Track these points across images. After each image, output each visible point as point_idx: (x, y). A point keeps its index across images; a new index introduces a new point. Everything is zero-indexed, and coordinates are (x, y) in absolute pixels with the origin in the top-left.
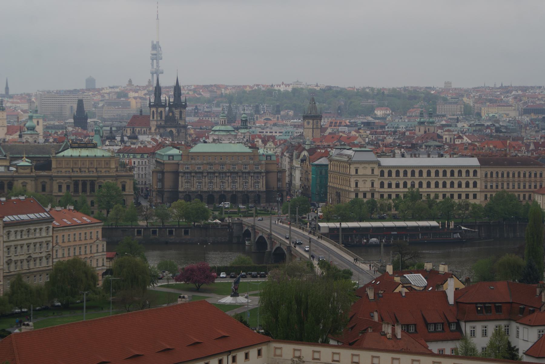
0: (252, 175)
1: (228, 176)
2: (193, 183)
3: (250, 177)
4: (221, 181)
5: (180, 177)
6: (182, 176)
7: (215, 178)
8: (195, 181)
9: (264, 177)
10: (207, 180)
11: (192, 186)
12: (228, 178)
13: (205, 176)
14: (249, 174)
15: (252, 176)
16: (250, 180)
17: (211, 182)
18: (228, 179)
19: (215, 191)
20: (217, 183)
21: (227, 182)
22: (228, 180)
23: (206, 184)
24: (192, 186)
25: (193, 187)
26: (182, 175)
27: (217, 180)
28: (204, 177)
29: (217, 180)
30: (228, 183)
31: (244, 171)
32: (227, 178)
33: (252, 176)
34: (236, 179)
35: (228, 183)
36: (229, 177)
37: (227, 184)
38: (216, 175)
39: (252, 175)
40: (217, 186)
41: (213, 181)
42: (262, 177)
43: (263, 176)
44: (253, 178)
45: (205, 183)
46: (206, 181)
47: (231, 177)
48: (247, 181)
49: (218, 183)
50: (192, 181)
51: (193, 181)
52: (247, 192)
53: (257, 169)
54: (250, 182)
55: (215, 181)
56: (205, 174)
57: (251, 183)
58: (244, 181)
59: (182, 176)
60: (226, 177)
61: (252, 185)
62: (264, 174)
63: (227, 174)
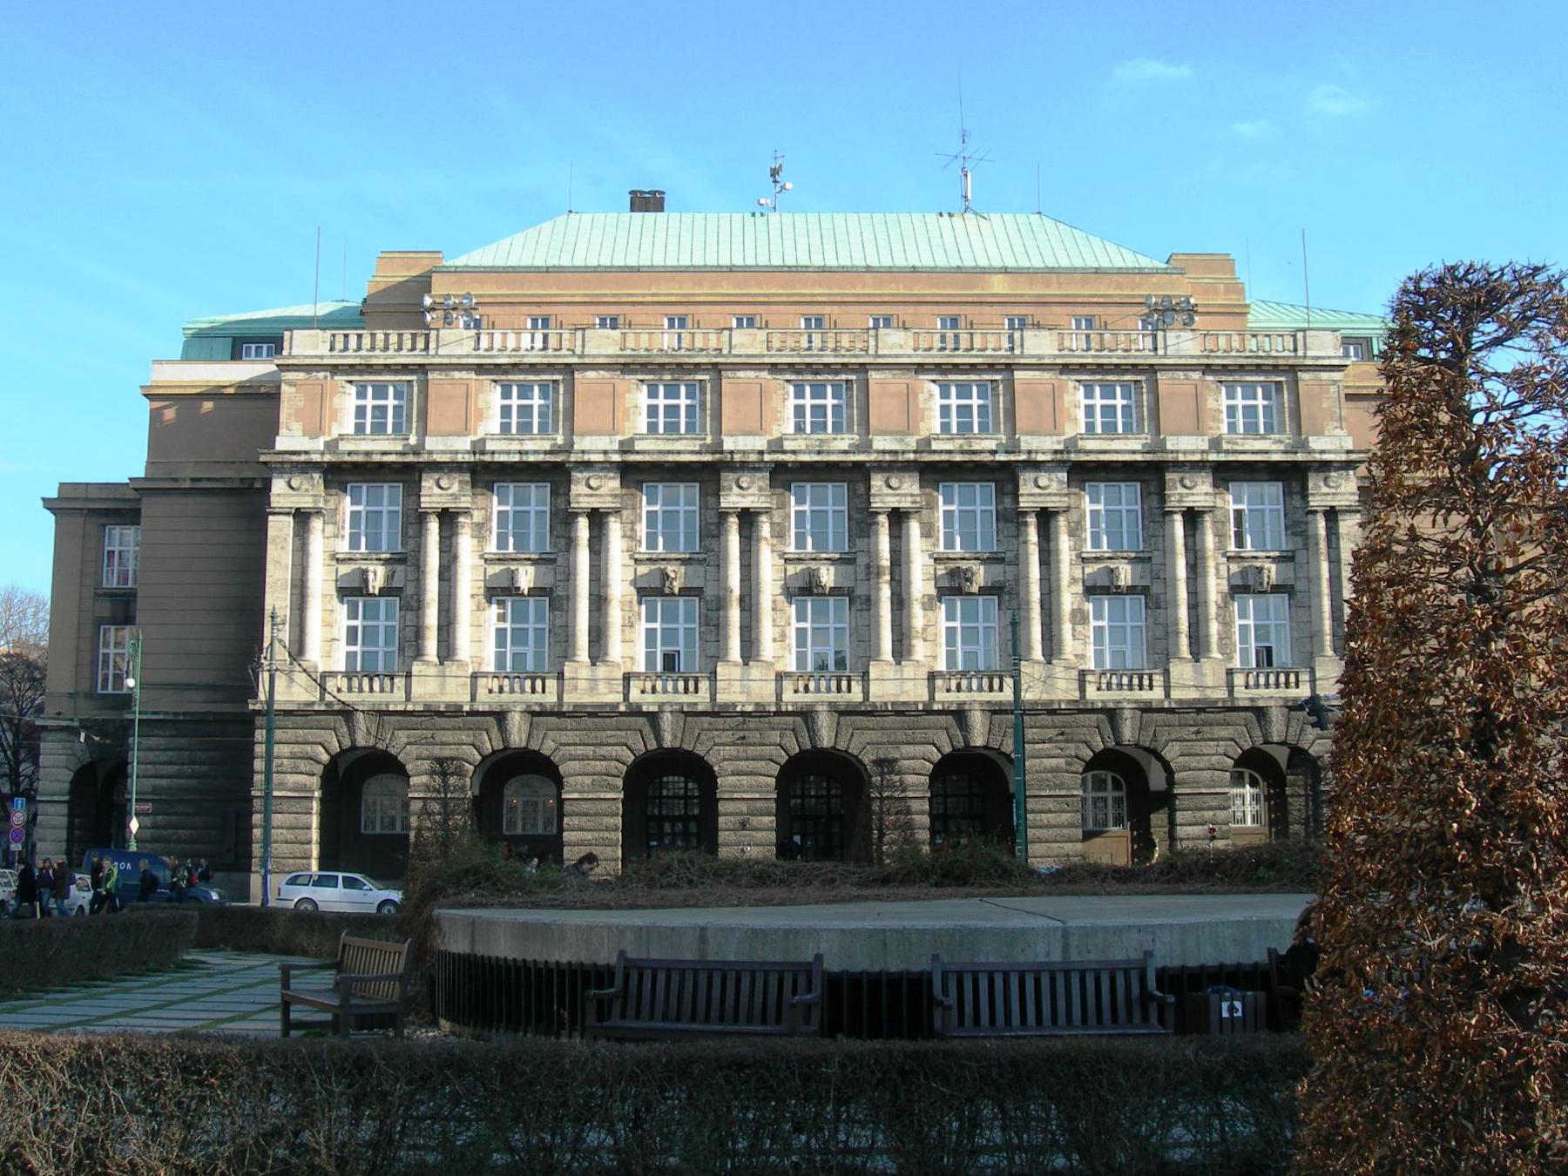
0: (1199, 492)
1: (898, 518)
5: (280, 529)
6: (302, 518)
11: (431, 645)
14: (1162, 486)
19: (719, 712)
24: (431, 645)
25: (447, 651)
26: (306, 502)
28: (583, 528)
35: (900, 602)
36: (914, 527)
38: (733, 499)
39: (1199, 492)
43: (1332, 514)
52: (1146, 708)
63: (877, 482)
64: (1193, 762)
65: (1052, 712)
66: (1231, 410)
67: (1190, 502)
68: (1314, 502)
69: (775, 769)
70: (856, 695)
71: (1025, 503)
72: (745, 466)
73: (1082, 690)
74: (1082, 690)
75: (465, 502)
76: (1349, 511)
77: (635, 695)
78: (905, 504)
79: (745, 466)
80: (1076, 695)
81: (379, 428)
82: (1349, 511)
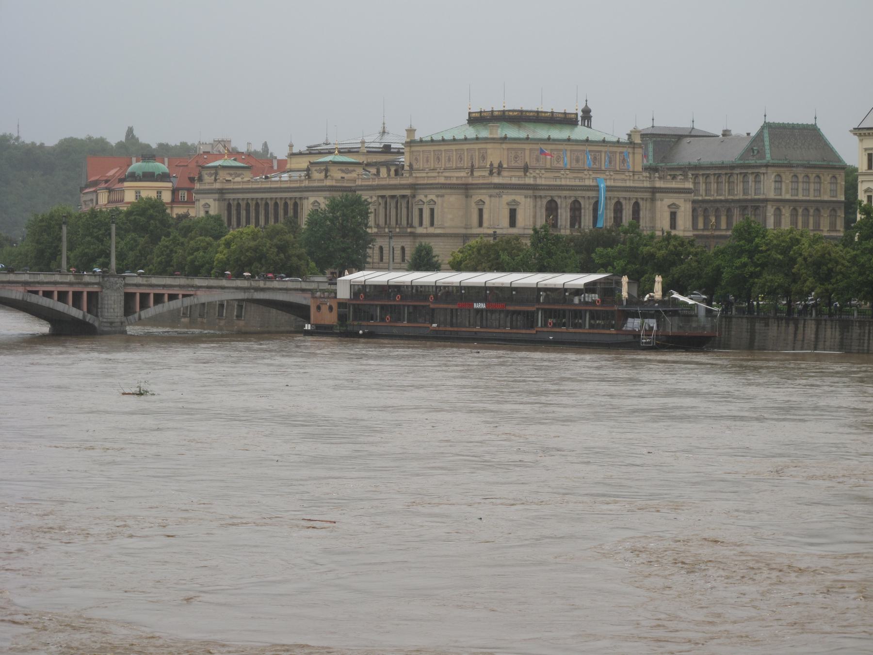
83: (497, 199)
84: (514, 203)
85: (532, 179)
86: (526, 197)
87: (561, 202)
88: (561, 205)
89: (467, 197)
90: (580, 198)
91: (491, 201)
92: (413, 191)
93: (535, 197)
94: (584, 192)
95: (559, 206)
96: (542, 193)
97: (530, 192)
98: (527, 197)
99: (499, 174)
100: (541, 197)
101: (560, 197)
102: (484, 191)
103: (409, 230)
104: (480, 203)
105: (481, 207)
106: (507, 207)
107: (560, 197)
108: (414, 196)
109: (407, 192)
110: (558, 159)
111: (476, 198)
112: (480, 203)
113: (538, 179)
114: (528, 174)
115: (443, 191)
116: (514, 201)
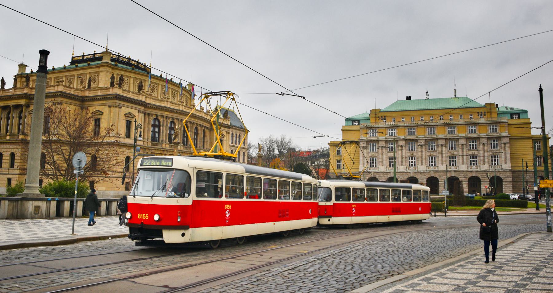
1: (442, 145)
2: (382, 158)
3: (481, 146)
4: (429, 154)
7: (419, 149)
8: (384, 154)
9: (508, 145)
10: (406, 153)
12: (442, 148)
13: (402, 146)
15: (484, 144)
16: (481, 152)
17: (412, 158)
18: (442, 151)
20: (421, 157)
21: (440, 156)
22: (442, 153)
23: (404, 159)
26: (365, 145)
27: (422, 152)
28: (400, 148)
29: (422, 152)
30: (442, 157)
31: (469, 135)
32: (440, 149)
33: (484, 144)
34: (456, 151)
35: (442, 157)
36: (444, 148)
37: (440, 158)
40: (422, 161)
41: (415, 154)
42: (503, 145)
43: (505, 144)
44: (486, 148)
45: (402, 157)
46: (404, 154)
47: (446, 147)
48: (476, 153)
49: (424, 157)
50: (380, 156)
51: (382, 154)
53: (493, 131)
54: (482, 155)
55: (420, 154)
56: (402, 143)
57: (484, 157)
58: (470, 153)
59: (363, 147)
60: (438, 146)
61: (486, 160)
62: (507, 140)
64: (483, 178)
65: (464, 172)
66: (490, 129)
67: (484, 142)
68: (502, 142)
69: (426, 179)
70: (437, 170)
71: (460, 143)
72: (421, 139)
73: (468, 168)
74: (468, 168)
75: (385, 145)
76: (508, 143)
77: (407, 170)
78: (443, 144)
79: (421, 139)
80: (467, 169)
81: (373, 136)
82: (508, 143)
83: (117, 109)
84: (129, 116)
85: (144, 97)
86: (139, 112)
87: (163, 121)
88: (163, 123)
89: (82, 108)
90: (175, 120)
91: (110, 112)
92: (27, 101)
93: (145, 114)
94: (179, 115)
95: (162, 124)
96: (150, 111)
97: (142, 108)
98: (140, 112)
99: (120, 85)
100: (149, 114)
101: (163, 116)
102: (104, 102)
103: (21, 137)
104: (97, 114)
105: (98, 117)
106: (124, 118)
107: (163, 116)
108: (28, 106)
109: (22, 102)
110: (153, 90)
111: (92, 109)
112: (97, 114)
113: (147, 99)
114: (141, 92)
115: (62, 99)
116: (130, 114)
